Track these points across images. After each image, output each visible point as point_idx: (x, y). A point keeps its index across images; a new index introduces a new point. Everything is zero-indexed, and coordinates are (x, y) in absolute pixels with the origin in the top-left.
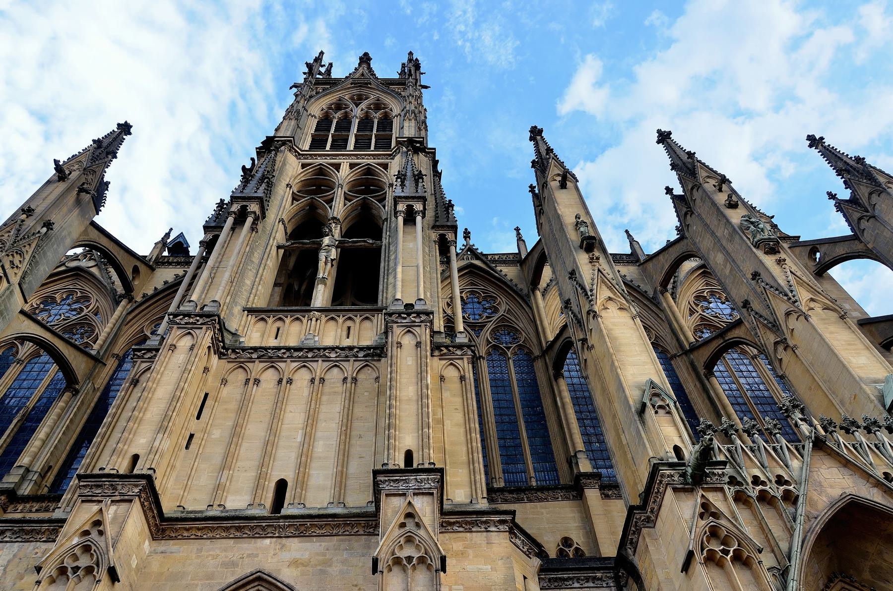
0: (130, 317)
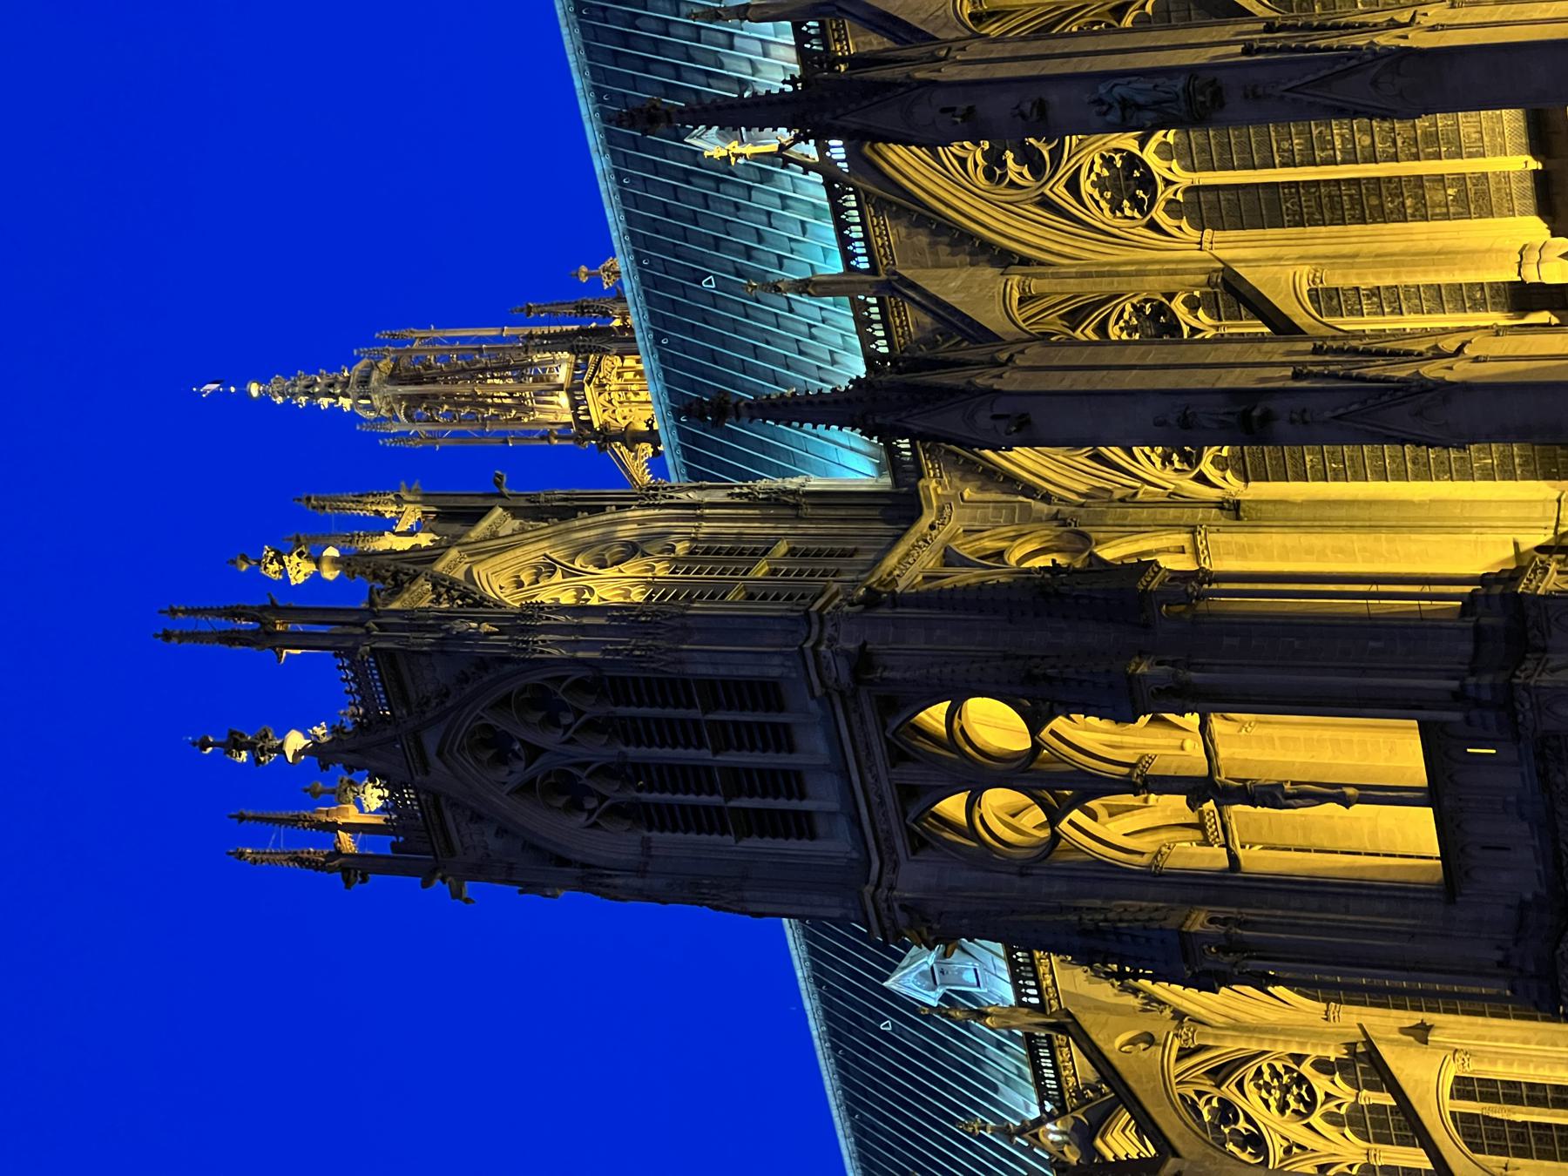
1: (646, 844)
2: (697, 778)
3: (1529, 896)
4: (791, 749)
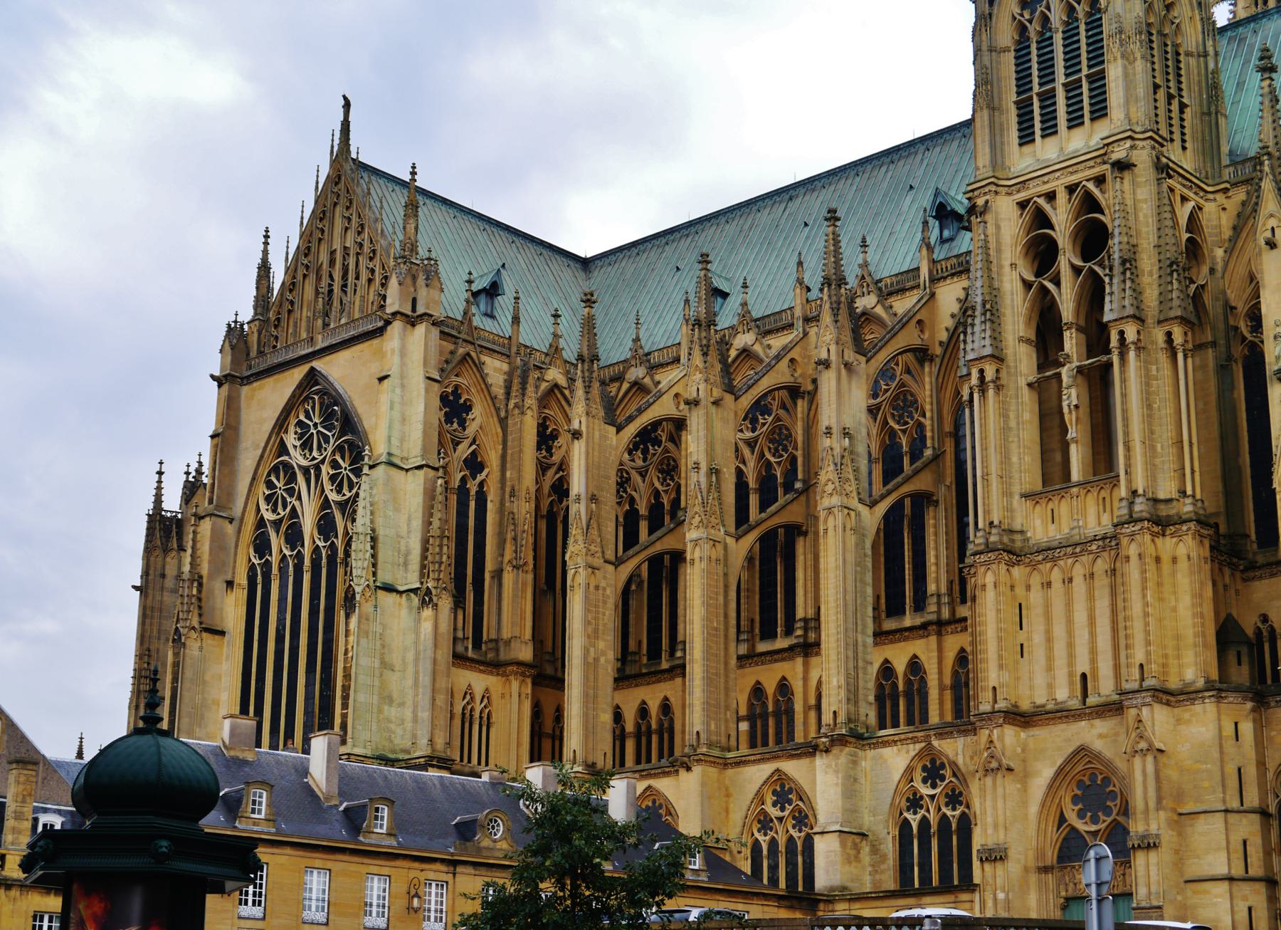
0: (940, 380)
1: (1006, 50)
2: (1047, 73)
3: (1029, 535)
4: (1069, 128)
